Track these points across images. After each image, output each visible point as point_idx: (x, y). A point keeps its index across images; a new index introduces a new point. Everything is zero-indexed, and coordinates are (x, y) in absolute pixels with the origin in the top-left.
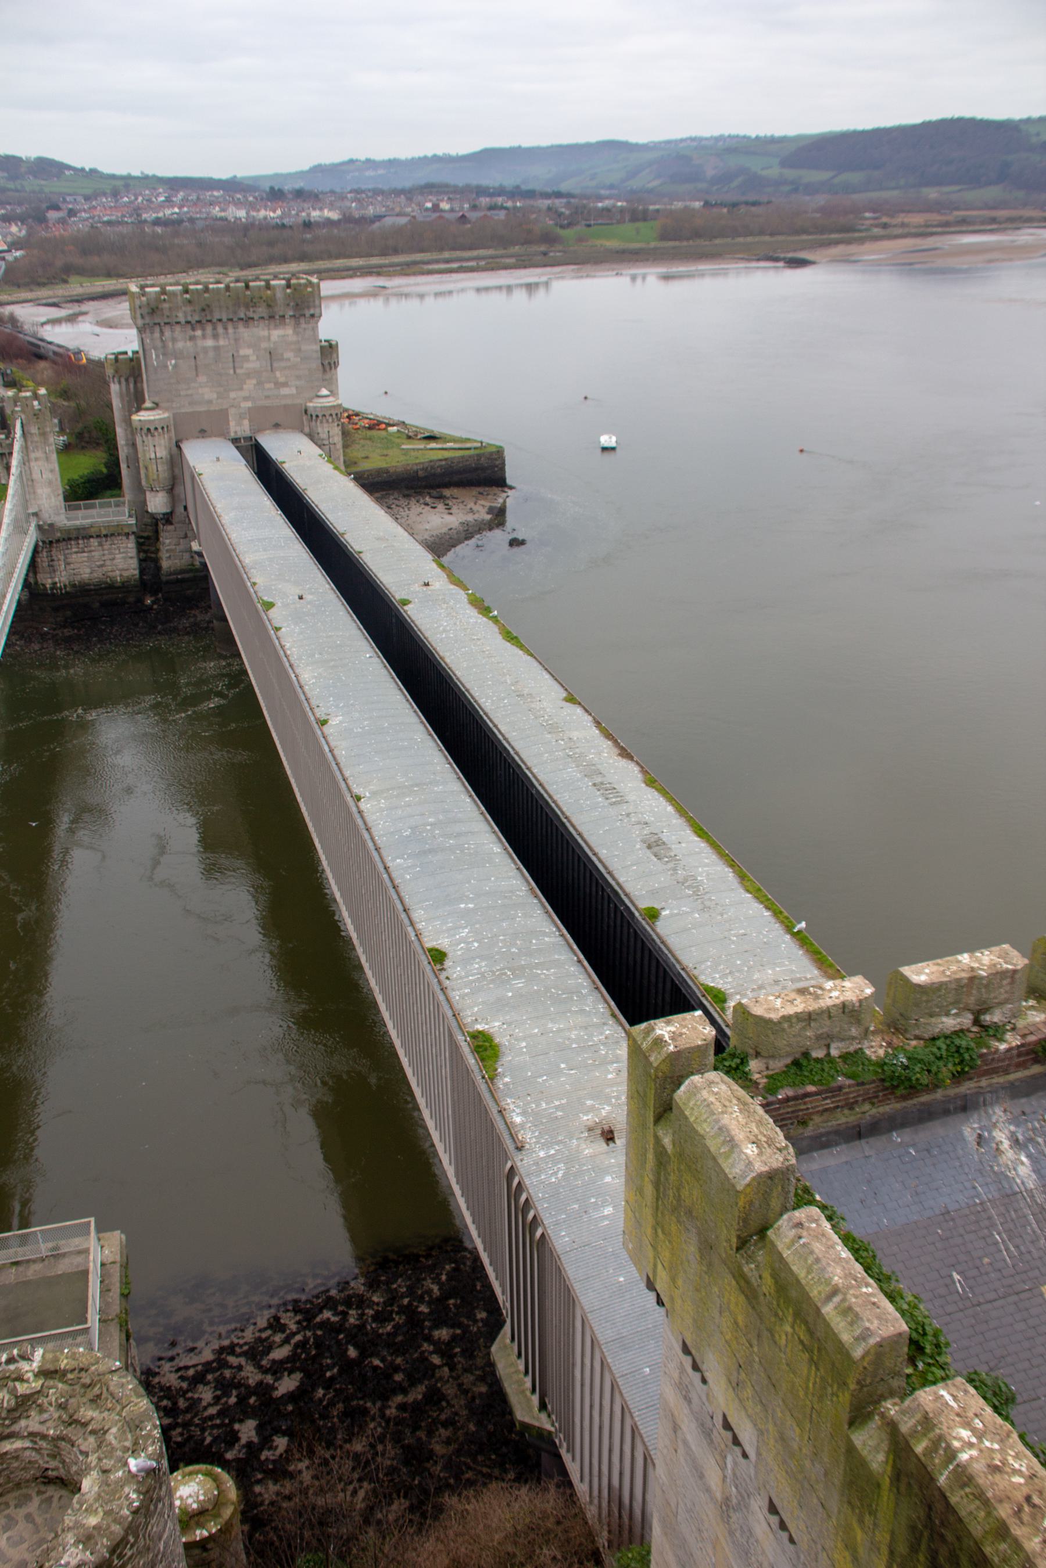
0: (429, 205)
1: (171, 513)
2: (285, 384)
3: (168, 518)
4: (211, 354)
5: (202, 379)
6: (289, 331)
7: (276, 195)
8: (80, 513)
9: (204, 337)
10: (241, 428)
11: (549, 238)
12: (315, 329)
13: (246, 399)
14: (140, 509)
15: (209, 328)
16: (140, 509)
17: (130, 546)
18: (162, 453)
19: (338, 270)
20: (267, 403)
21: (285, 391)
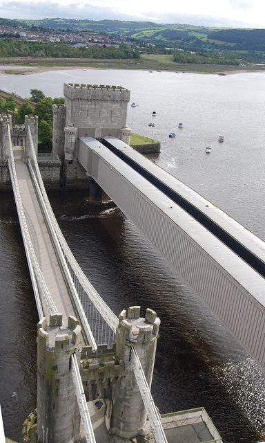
0: (90, 39)
1: (72, 161)
2: (114, 122)
3: (71, 162)
4: (93, 110)
5: (89, 118)
6: (118, 105)
7: (34, 28)
8: (43, 158)
9: (92, 104)
10: (98, 135)
11: (136, 56)
12: (126, 105)
13: (101, 125)
14: (62, 157)
15: (93, 102)
16: (62, 157)
17: (58, 170)
18: (73, 141)
19: (73, 62)
20: (108, 127)
21: (114, 124)
